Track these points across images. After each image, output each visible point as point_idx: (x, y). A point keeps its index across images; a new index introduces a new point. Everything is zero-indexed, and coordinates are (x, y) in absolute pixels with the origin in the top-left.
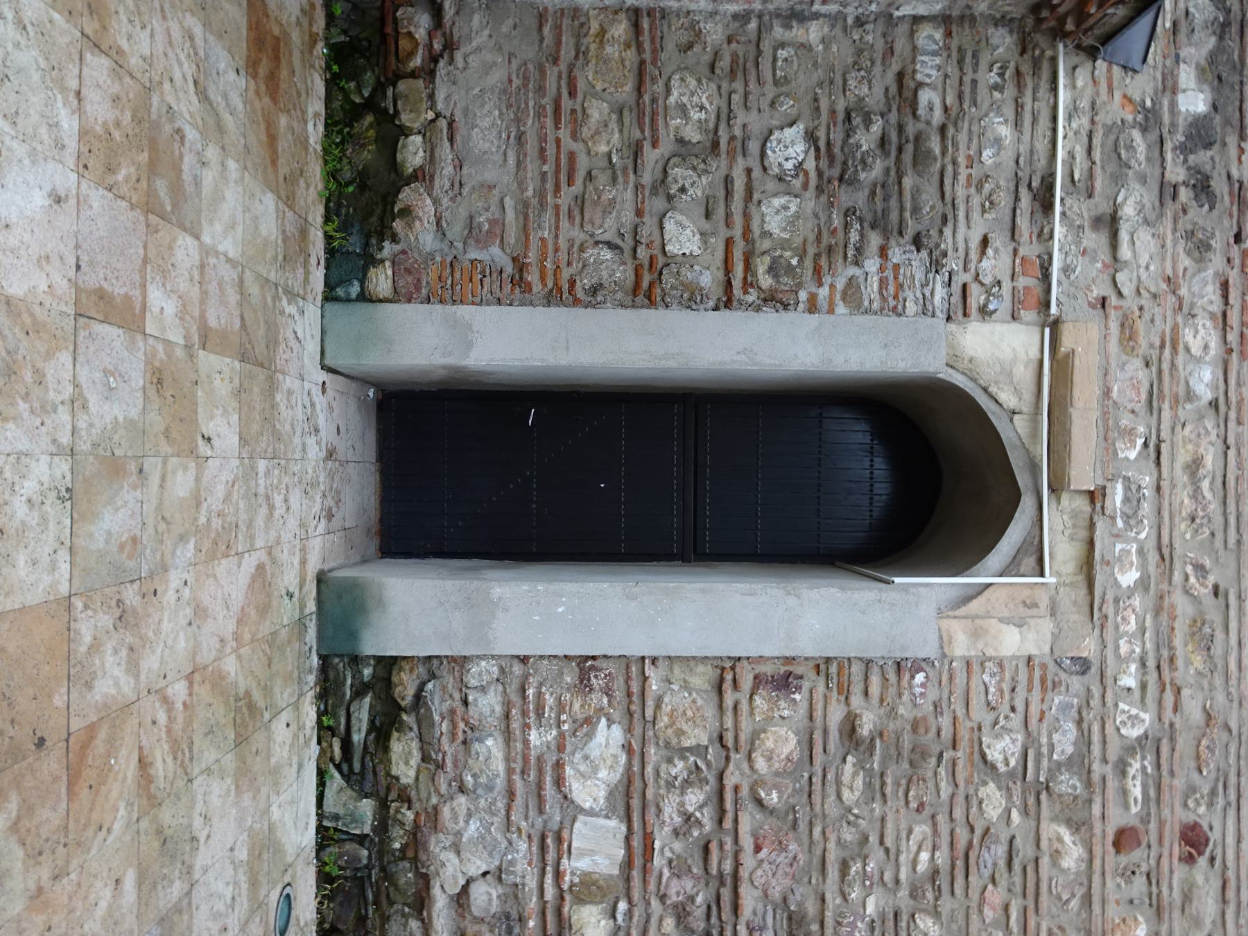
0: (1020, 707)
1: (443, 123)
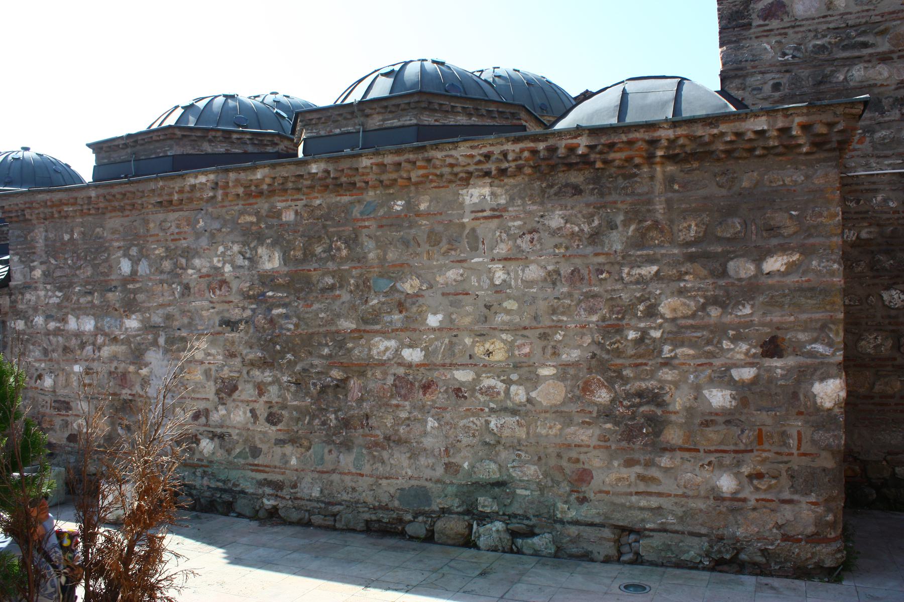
1: (889, 458)
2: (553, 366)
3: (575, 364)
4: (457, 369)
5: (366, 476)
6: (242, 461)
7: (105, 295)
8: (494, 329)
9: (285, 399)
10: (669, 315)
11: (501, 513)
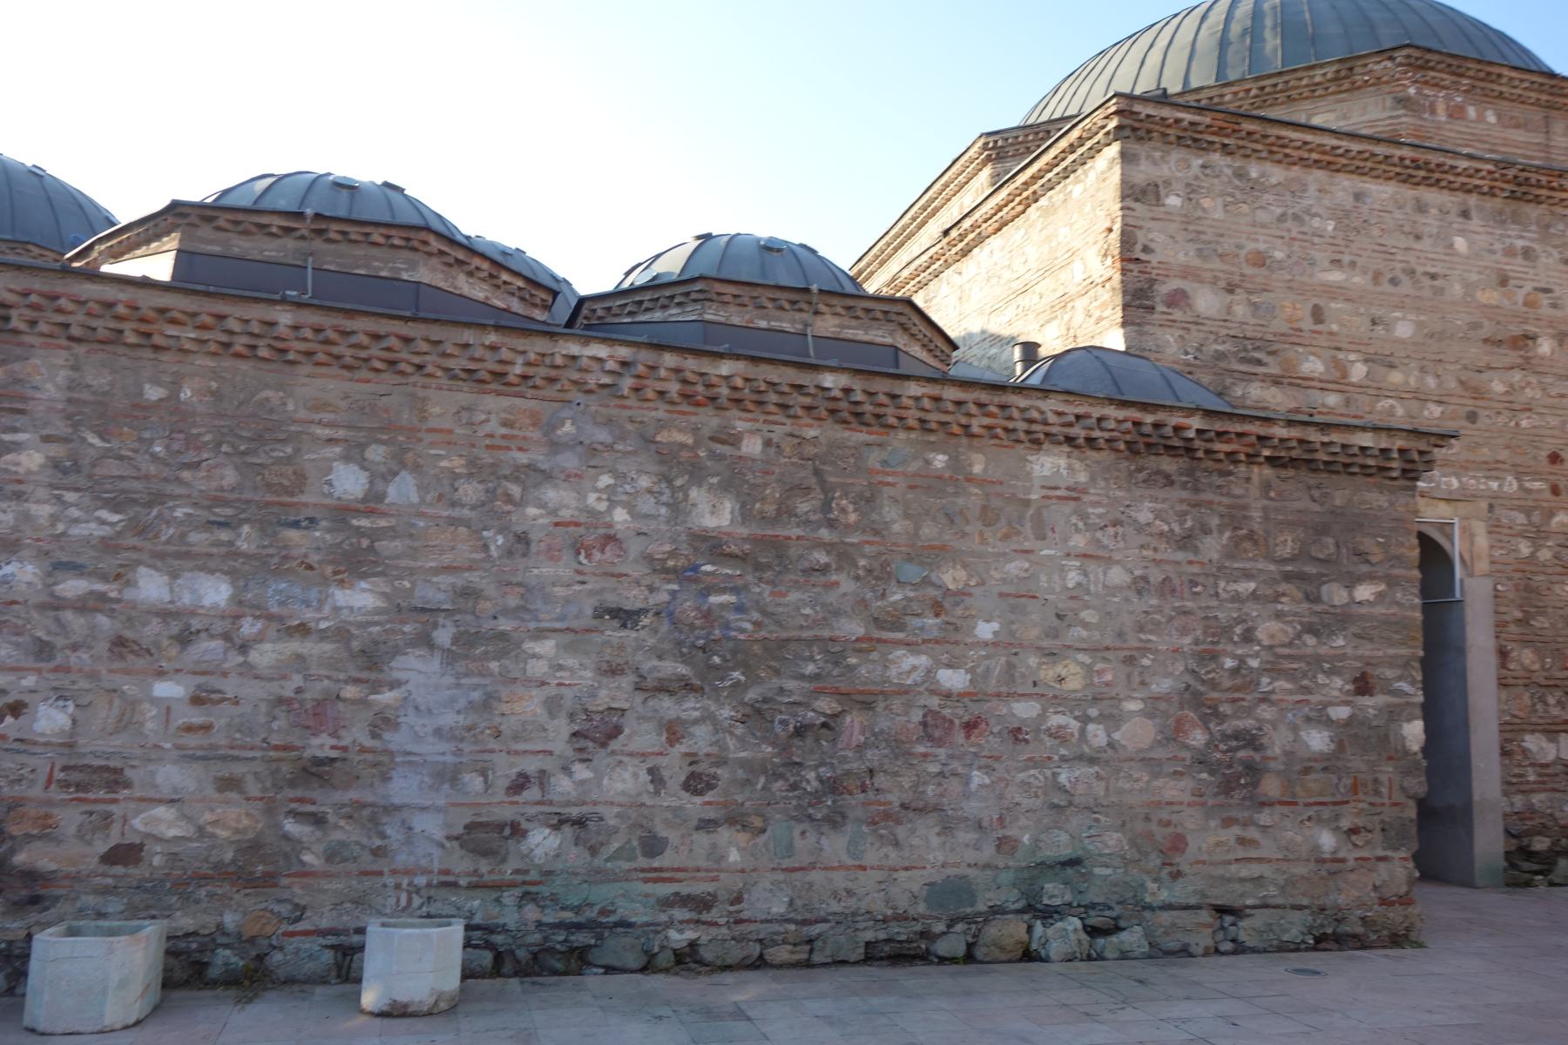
0: (1507, 538)
2: (1141, 699)
3: (1165, 698)
4: (1018, 701)
5: (872, 868)
6: (626, 865)
7: (275, 534)
8: (1069, 647)
9: (723, 748)
10: (1266, 642)
11: (1075, 904)
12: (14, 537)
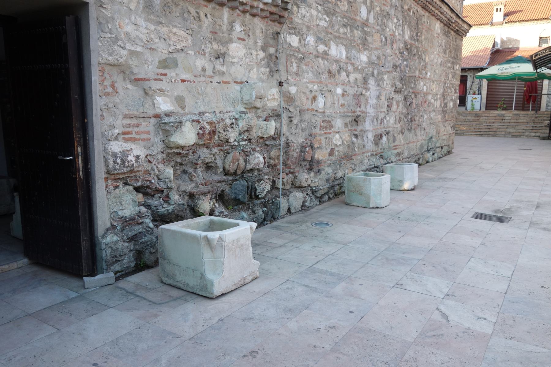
12: (309, 24)
